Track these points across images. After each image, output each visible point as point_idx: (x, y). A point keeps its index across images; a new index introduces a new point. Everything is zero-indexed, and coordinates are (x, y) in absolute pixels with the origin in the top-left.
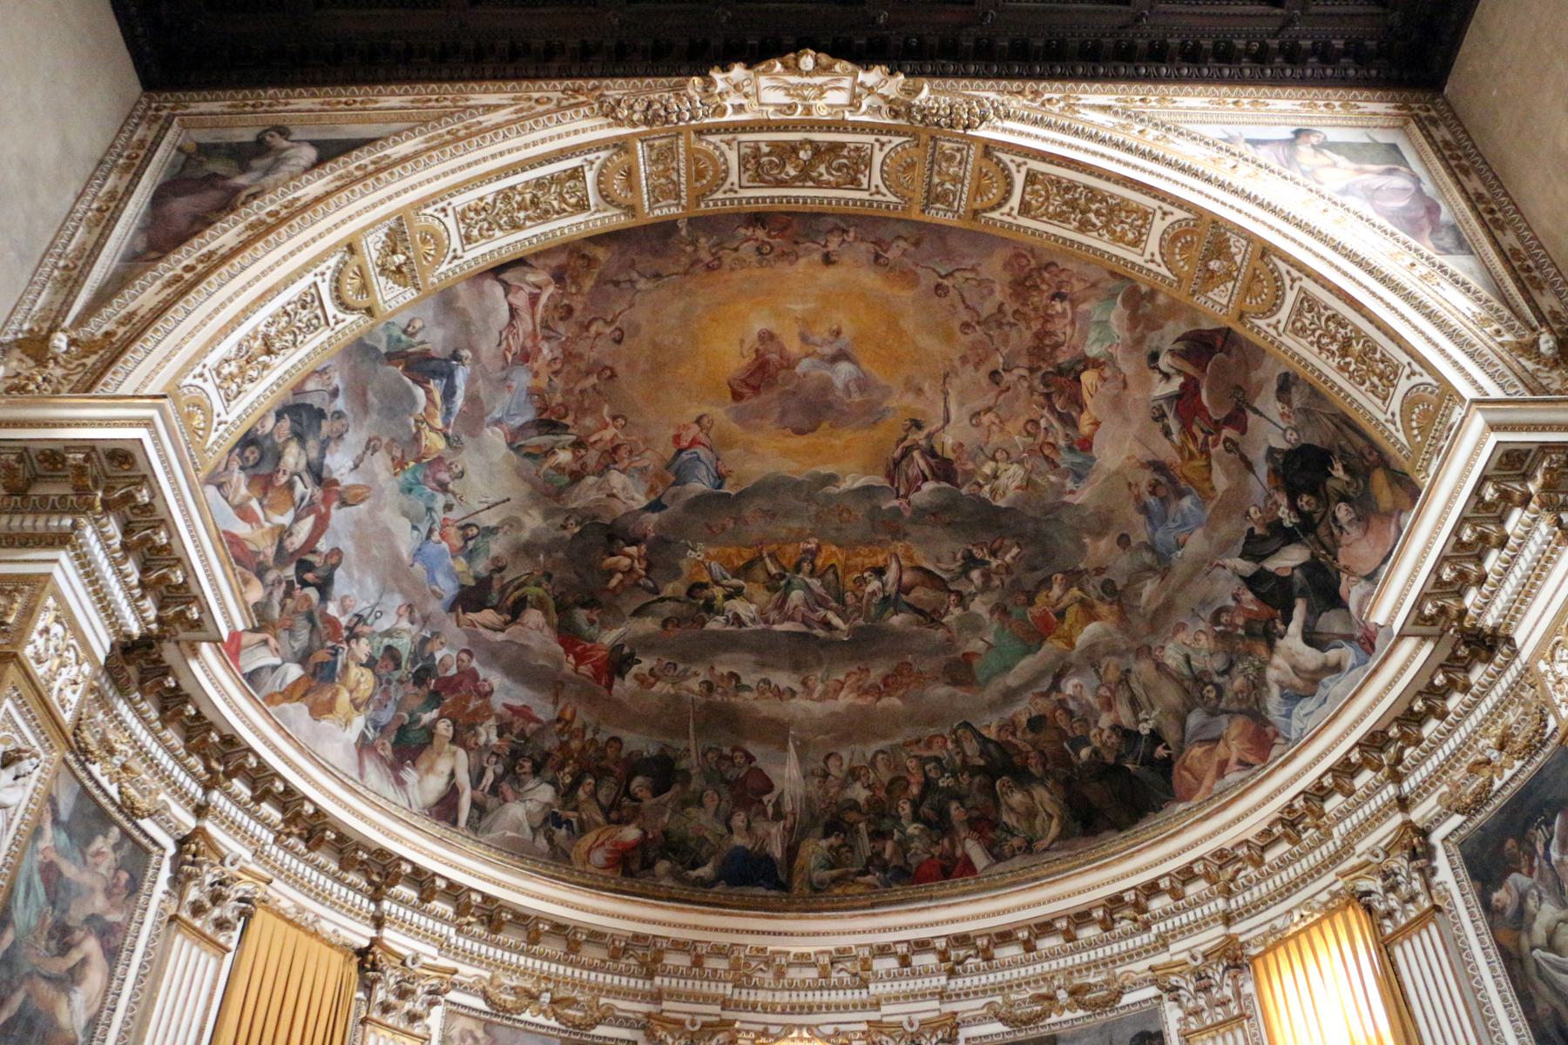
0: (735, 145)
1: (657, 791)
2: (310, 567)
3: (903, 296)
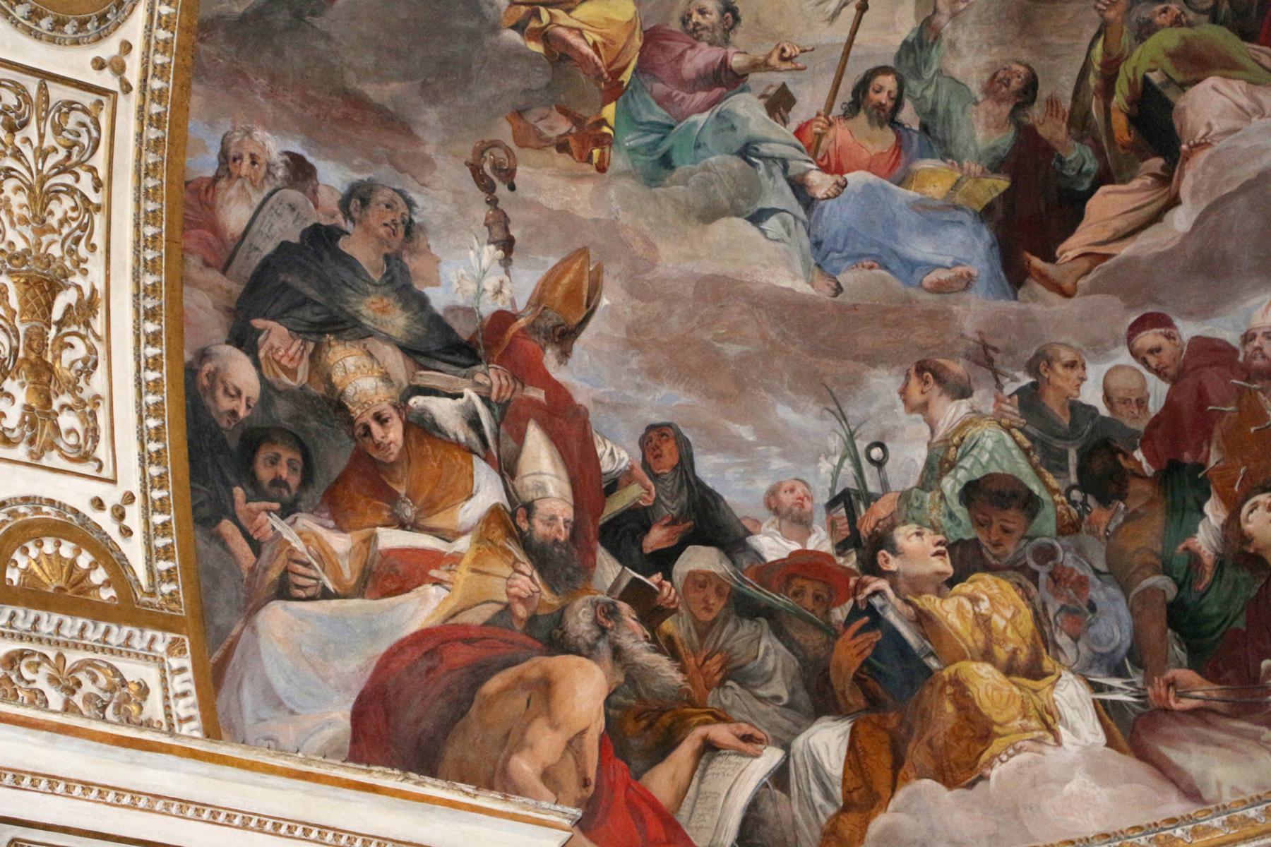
2: (638, 519)
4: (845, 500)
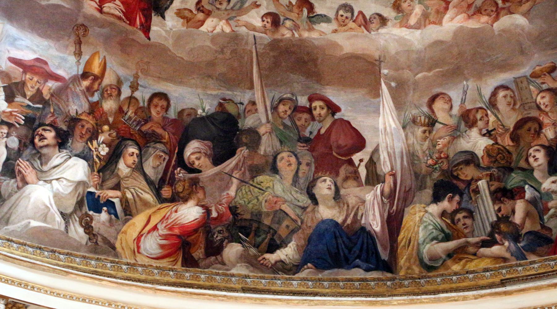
1: (217, 160)
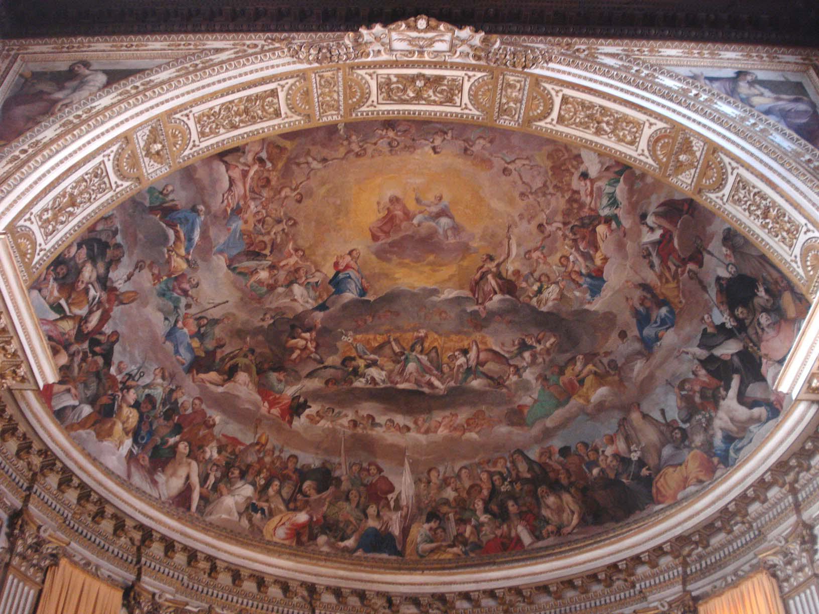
0: (375, 76)
1: (319, 491)
2: (98, 343)
3: (484, 177)
4: (130, 376)
